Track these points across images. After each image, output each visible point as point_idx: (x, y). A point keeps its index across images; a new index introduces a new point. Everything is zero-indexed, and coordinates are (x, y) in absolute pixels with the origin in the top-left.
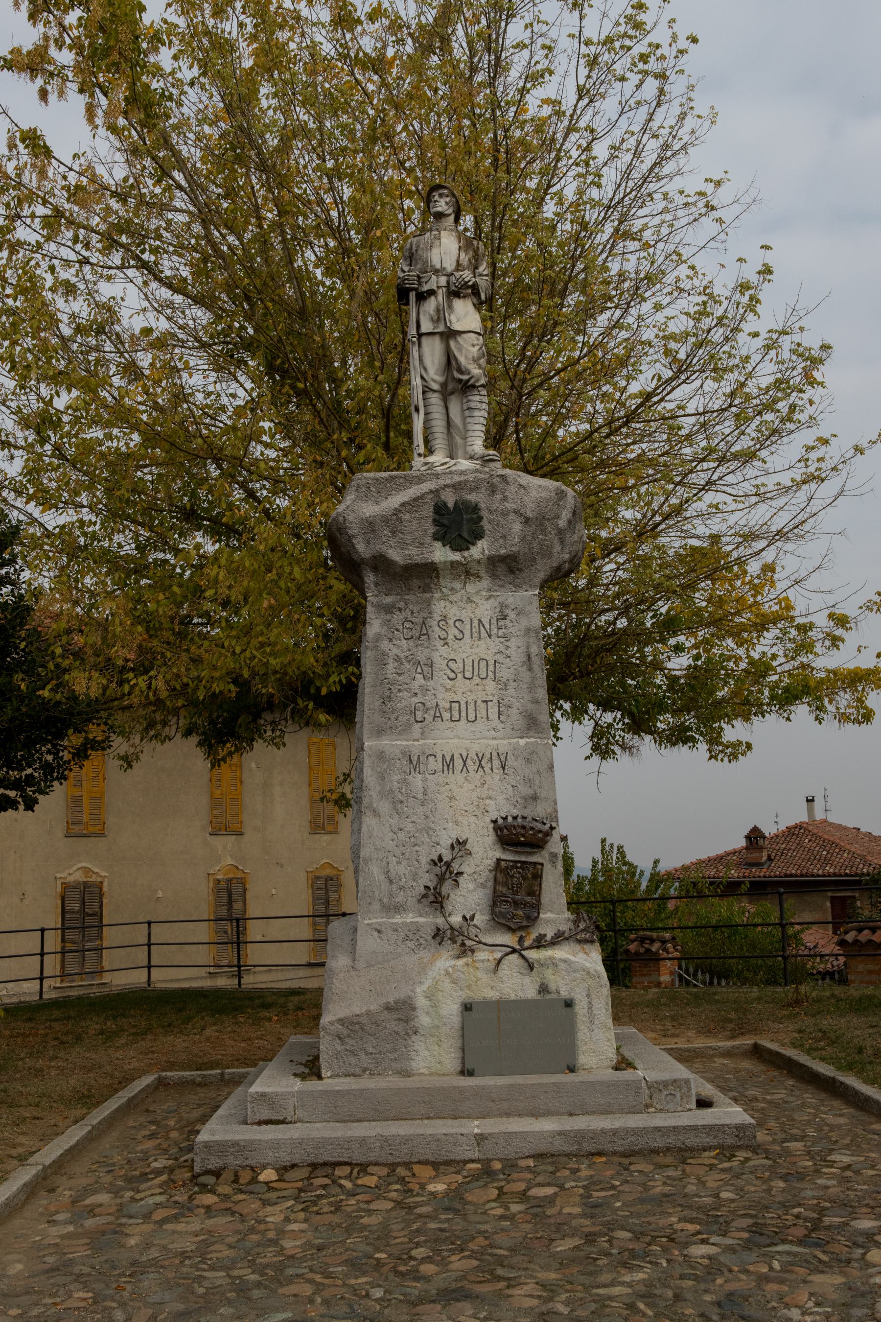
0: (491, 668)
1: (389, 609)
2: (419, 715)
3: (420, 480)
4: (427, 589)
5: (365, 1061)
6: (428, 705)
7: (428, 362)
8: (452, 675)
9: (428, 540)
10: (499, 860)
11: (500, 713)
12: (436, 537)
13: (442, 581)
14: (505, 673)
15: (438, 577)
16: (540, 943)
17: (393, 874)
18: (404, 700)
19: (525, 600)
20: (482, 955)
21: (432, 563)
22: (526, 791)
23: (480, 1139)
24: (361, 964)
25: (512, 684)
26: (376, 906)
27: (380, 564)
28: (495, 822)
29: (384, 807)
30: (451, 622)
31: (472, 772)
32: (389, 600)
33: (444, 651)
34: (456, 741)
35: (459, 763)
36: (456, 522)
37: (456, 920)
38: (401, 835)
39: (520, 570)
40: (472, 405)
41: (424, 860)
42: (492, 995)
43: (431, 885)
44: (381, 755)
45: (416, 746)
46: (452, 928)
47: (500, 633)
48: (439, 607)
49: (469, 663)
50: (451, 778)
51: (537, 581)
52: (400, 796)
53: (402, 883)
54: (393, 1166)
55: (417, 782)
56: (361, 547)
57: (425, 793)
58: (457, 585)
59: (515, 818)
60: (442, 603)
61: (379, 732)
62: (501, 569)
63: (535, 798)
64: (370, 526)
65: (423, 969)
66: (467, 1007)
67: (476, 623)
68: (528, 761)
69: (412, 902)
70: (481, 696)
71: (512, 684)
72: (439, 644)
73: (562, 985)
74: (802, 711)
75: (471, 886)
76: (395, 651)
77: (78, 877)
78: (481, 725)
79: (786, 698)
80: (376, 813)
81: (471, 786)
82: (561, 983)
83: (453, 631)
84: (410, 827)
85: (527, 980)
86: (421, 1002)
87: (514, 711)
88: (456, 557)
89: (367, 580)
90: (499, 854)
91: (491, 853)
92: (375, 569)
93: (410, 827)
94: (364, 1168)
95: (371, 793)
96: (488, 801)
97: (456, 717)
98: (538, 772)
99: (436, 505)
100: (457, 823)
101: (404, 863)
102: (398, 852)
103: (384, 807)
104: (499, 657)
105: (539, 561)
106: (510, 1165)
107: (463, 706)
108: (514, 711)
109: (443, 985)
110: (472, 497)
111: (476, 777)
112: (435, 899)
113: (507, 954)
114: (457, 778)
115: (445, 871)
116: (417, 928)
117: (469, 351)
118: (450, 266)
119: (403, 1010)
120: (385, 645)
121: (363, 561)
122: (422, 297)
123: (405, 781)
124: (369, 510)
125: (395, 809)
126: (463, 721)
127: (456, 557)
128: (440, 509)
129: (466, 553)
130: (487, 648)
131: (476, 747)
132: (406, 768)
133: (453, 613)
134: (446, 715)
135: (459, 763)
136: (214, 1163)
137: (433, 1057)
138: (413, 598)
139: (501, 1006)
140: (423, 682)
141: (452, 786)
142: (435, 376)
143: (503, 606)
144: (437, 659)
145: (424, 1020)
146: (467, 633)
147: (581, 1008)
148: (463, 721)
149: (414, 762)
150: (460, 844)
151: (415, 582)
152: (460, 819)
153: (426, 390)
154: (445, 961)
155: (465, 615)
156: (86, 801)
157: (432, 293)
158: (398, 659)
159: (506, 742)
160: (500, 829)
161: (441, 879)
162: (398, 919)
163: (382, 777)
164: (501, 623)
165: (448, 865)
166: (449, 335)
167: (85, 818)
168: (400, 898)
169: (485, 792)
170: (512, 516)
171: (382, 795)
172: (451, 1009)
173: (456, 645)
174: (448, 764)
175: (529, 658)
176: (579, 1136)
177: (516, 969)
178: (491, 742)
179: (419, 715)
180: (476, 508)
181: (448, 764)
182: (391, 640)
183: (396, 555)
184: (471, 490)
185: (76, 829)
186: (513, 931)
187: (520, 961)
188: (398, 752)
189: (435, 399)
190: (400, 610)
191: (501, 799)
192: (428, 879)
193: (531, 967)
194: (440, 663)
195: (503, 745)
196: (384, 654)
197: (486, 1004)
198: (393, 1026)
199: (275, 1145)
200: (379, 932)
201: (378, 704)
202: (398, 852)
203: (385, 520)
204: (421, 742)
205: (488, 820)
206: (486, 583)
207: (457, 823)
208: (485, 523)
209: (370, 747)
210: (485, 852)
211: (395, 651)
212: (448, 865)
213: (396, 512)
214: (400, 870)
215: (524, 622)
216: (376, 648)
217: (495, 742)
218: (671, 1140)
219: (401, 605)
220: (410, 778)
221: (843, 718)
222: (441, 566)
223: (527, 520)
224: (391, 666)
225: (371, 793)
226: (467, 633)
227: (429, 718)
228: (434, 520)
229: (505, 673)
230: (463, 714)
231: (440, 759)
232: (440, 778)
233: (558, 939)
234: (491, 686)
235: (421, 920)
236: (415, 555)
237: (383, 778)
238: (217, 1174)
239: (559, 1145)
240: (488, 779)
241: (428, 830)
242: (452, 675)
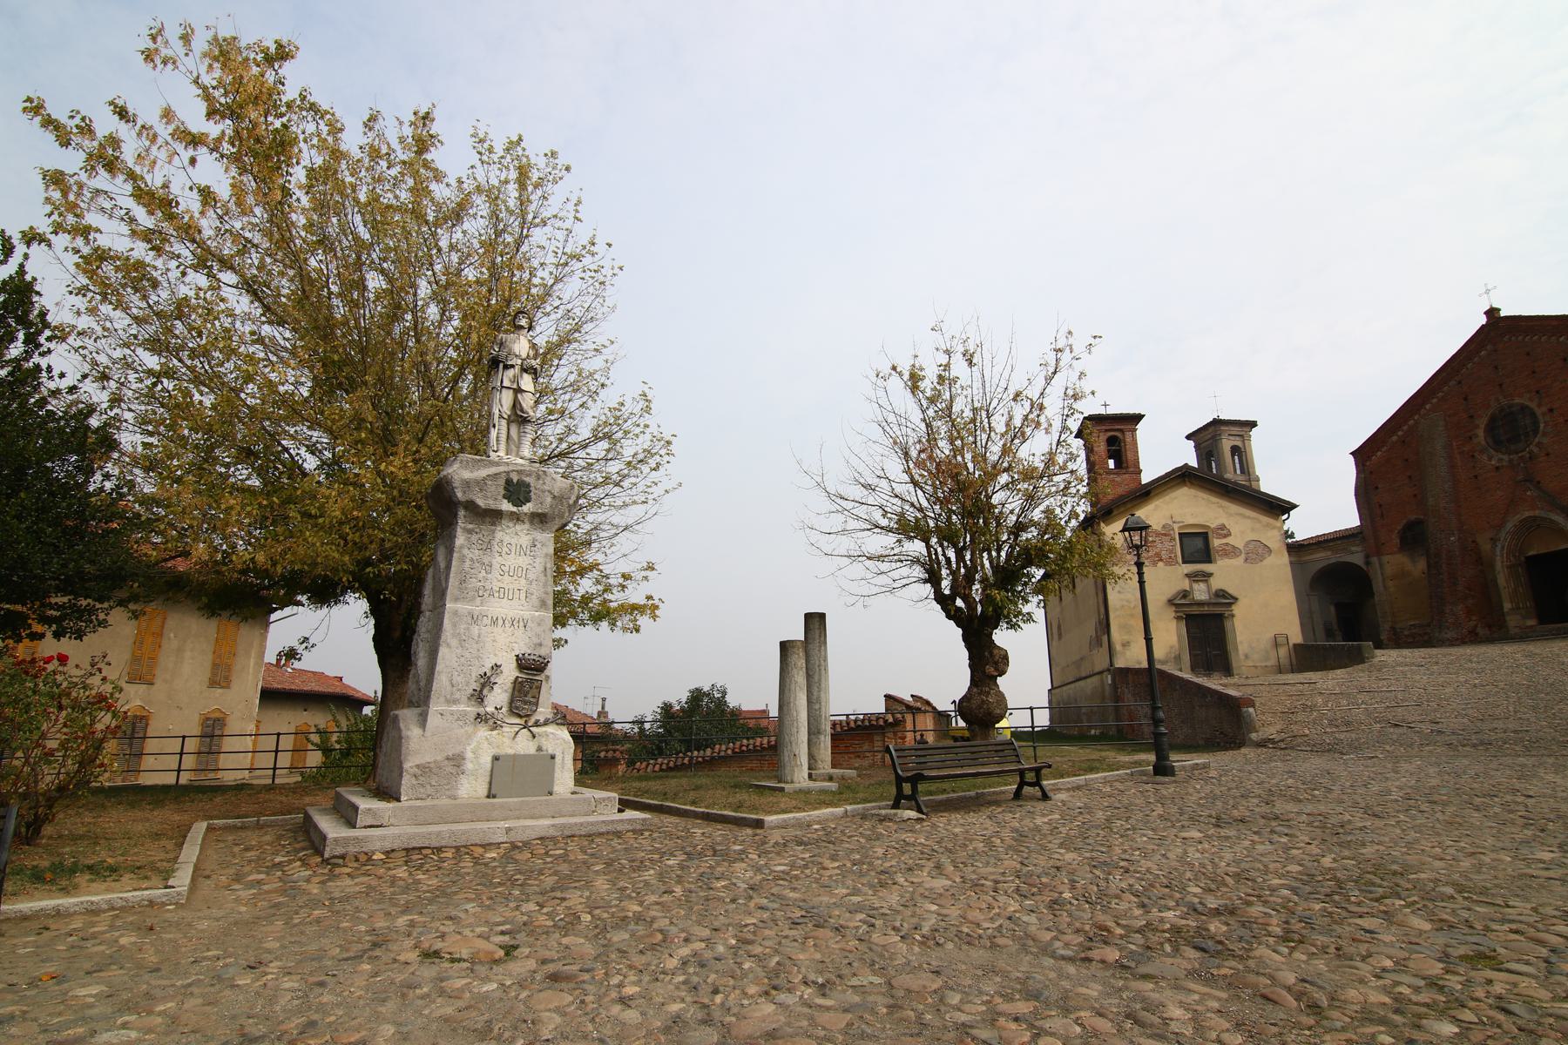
3: (498, 464)
4: (493, 524)
5: (430, 790)
12: (505, 497)
14: (531, 576)
16: (537, 724)
18: (473, 583)
19: (546, 539)
20: (506, 729)
22: (536, 641)
23: (508, 830)
24: (428, 733)
27: (471, 506)
29: (454, 642)
36: (517, 491)
37: (490, 709)
42: (511, 752)
44: (456, 613)
45: (477, 610)
48: (499, 535)
54: (457, 848)
55: (475, 630)
56: (459, 495)
61: (456, 600)
64: (467, 484)
65: (469, 737)
66: (496, 758)
69: (464, 699)
70: (517, 586)
73: (550, 748)
74: (604, 624)
79: (597, 618)
86: (469, 755)
88: (514, 509)
92: (466, 508)
94: (439, 849)
103: (454, 642)
106: (526, 844)
109: (482, 747)
110: (527, 479)
111: (509, 630)
112: (479, 697)
114: (498, 630)
115: (486, 682)
116: (465, 714)
117: (527, 401)
118: (524, 355)
119: (457, 760)
120: (465, 551)
122: (506, 367)
124: (467, 475)
127: (514, 509)
128: (509, 482)
130: (523, 561)
131: (511, 614)
133: (507, 539)
136: (339, 851)
137: (472, 787)
139: (515, 758)
142: (507, 410)
143: (534, 540)
144: (494, 562)
145: (469, 766)
147: (558, 760)
149: (474, 619)
150: (496, 667)
153: (501, 417)
154: (483, 732)
155: (513, 541)
161: (483, 686)
162: (454, 708)
166: (518, 391)
168: (457, 696)
171: (453, 635)
172: (486, 760)
174: (494, 622)
176: (563, 826)
180: (528, 485)
181: (494, 622)
183: (481, 503)
186: (520, 716)
189: (504, 422)
194: (496, 566)
195: (527, 614)
197: (508, 756)
198: (449, 769)
199: (383, 838)
203: (477, 482)
206: (527, 526)
210: (510, 672)
213: (484, 479)
214: (457, 679)
215: (545, 550)
218: (610, 828)
221: (625, 629)
224: (468, 563)
229: (531, 576)
232: (489, 629)
233: (546, 723)
234: (523, 581)
236: (492, 504)
238: (343, 857)
239: (552, 832)
241: (478, 658)
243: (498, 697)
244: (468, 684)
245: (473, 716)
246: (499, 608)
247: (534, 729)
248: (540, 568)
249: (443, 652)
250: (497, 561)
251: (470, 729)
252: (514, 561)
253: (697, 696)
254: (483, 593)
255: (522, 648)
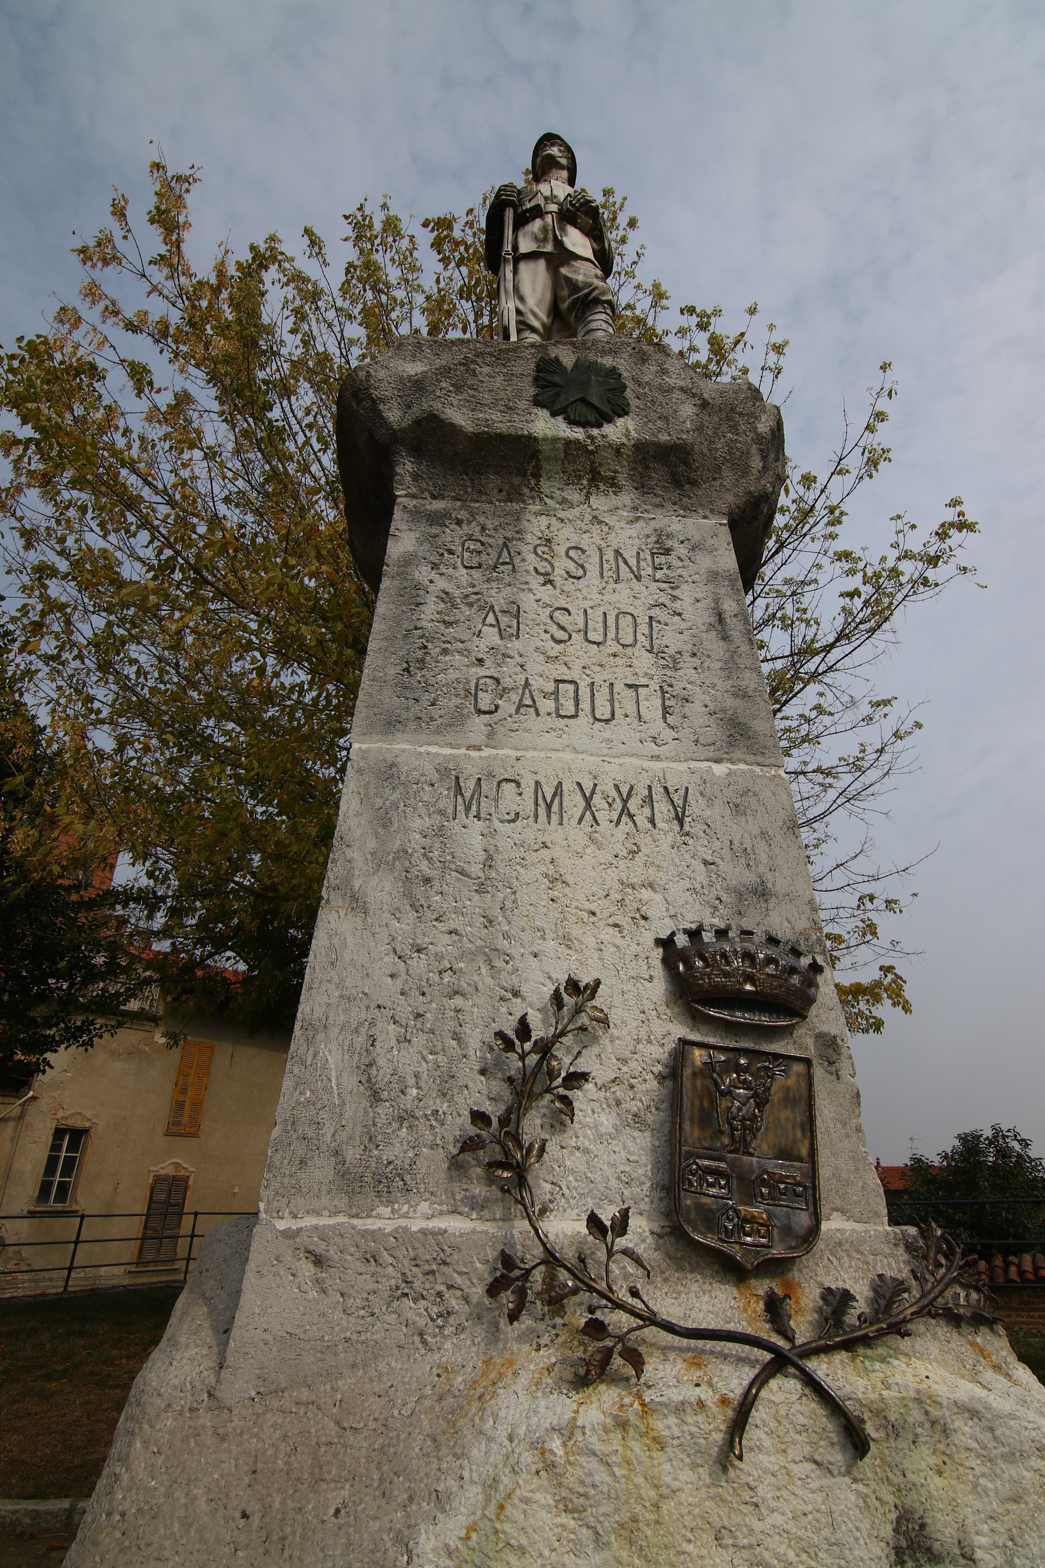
0: (643, 628)
1: (437, 519)
2: (485, 701)
4: (513, 495)
6: (507, 682)
7: (526, 289)
8: (561, 635)
9: (523, 404)
10: (684, 1042)
11: (666, 711)
12: (537, 402)
13: (545, 486)
15: (537, 476)
17: (382, 1075)
18: (456, 669)
20: (668, 1375)
21: (531, 439)
22: (736, 874)
24: (238, 1387)
25: (688, 663)
26: (322, 1170)
27: (432, 439)
28: (666, 944)
29: (381, 889)
30: (561, 550)
31: (604, 826)
32: (439, 505)
33: (545, 593)
34: (568, 756)
35: (574, 803)
37: (565, 1227)
38: (419, 964)
39: (694, 483)
40: (594, 325)
41: (477, 1038)
43: (494, 1111)
44: (388, 773)
45: (473, 762)
46: (551, 1259)
47: (659, 575)
48: (536, 525)
49: (596, 617)
50: (555, 834)
51: (724, 508)
52: (424, 866)
53: (408, 1102)
55: (470, 838)
56: (394, 415)
57: (489, 863)
58: (574, 495)
59: (721, 933)
60: (544, 521)
61: (391, 724)
62: (658, 475)
63: (762, 893)
67: (609, 555)
68: (737, 809)
69: (433, 1163)
70: (622, 675)
71: (688, 663)
72: (535, 582)
75: (607, 1121)
76: (441, 584)
77: (170, 1171)
78: (622, 730)
80: (357, 904)
81: (605, 856)
82: (971, 1508)
83: (562, 565)
84: (443, 944)
85: (846, 1494)
87: (696, 709)
89: (399, 470)
90: (680, 1030)
91: (659, 1028)
92: (417, 451)
93: (443, 944)
95: (352, 853)
96: (646, 894)
97: (569, 708)
98: (763, 834)
99: (539, 368)
100: (567, 941)
101: (419, 1041)
102: (404, 1012)
103: (381, 889)
104: (656, 612)
105: (726, 473)
107: (584, 692)
108: (696, 709)
112: (500, 1158)
113: (761, 1381)
114: (567, 835)
115: (536, 1073)
116: (440, 1253)
121: (396, 437)
123: (440, 832)
125: (409, 895)
126: (584, 719)
127: (578, 434)
129: (595, 432)
131: (615, 772)
132: (446, 803)
133: (565, 536)
134: (547, 705)
135: (574, 803)
138: (486, 507)
140: (496, 640)
141: (557, 852)
144: (527, 601)
146: (593, 569)
148: (584, 719)
149: (466, 794)
151: (493, 481)
152: (576, 931)
156: (187, 1106)
157: (537, 212)
158: (445, 597)
159: (683, 767)
160: (683, 956)
161: (524, 1091)
162: (382, 1221)
163: (383, 820)
164: (662, 559)
165: (545, 1048)
167: (185, 1120)
168: (396, 1151)
169: (637, 871)
170: (677, 395)
171: (379, 861)
173: (569, 585)
175: (720, 618)
177: (800, 1447)
178: (647, 764)
179: (485, 701)
181: (549, 803)
182: (435, 566)
183: (459, 416)
184: (603, 353)
185: (175, 1129)
186: (733, 1271)
187: (807, 1410)
188: (428, 768)
190: (459, 522)
191: (678, 891)
192: (482, 1094)
193: (855, 1439)
195: (677, 773)
196: (417, 587)
200: (319, 1261)
201: (392, 671)
202: (404, 1012)
204: (487, 752)
205: (648, 938)
206: (627, 498)
207: (567, 941)
208: (629, 394)
209: (364, 754)
210: (641, 1027)
211: (441, 584)
212: (545, 1048)
214: (404, 1060)
216: (402, 575)
217: (656, 766)
219: (463, 515)
220: (455, 826)
222: (545, 447)
223: (704, 405)
224: (431, 609)
225: (352, 853)
226: (593, 569)
227: (507, 707)
228: (536, 380)
229: (672, 640)
230: (585, 705)
231: (529, 791)
232: (528, 832)
234: (644, 661)
235: (456, 1225)
236: (499, 422)
237: (386, 823)
240: (644, 841)
241: (492, 956)
242: (561, 635)
243: (601, 1161)
244: (446, 1084)
245: (475, 1273)
246: (554, 751)
247: (834, 1371)
248: (698, 616)
249: (334, 930)
250: (536, 598)
251: (461, 1351)
252: (591, 597)
253: (970, 1143)
254: (490, 702)
255: (680, 903)
